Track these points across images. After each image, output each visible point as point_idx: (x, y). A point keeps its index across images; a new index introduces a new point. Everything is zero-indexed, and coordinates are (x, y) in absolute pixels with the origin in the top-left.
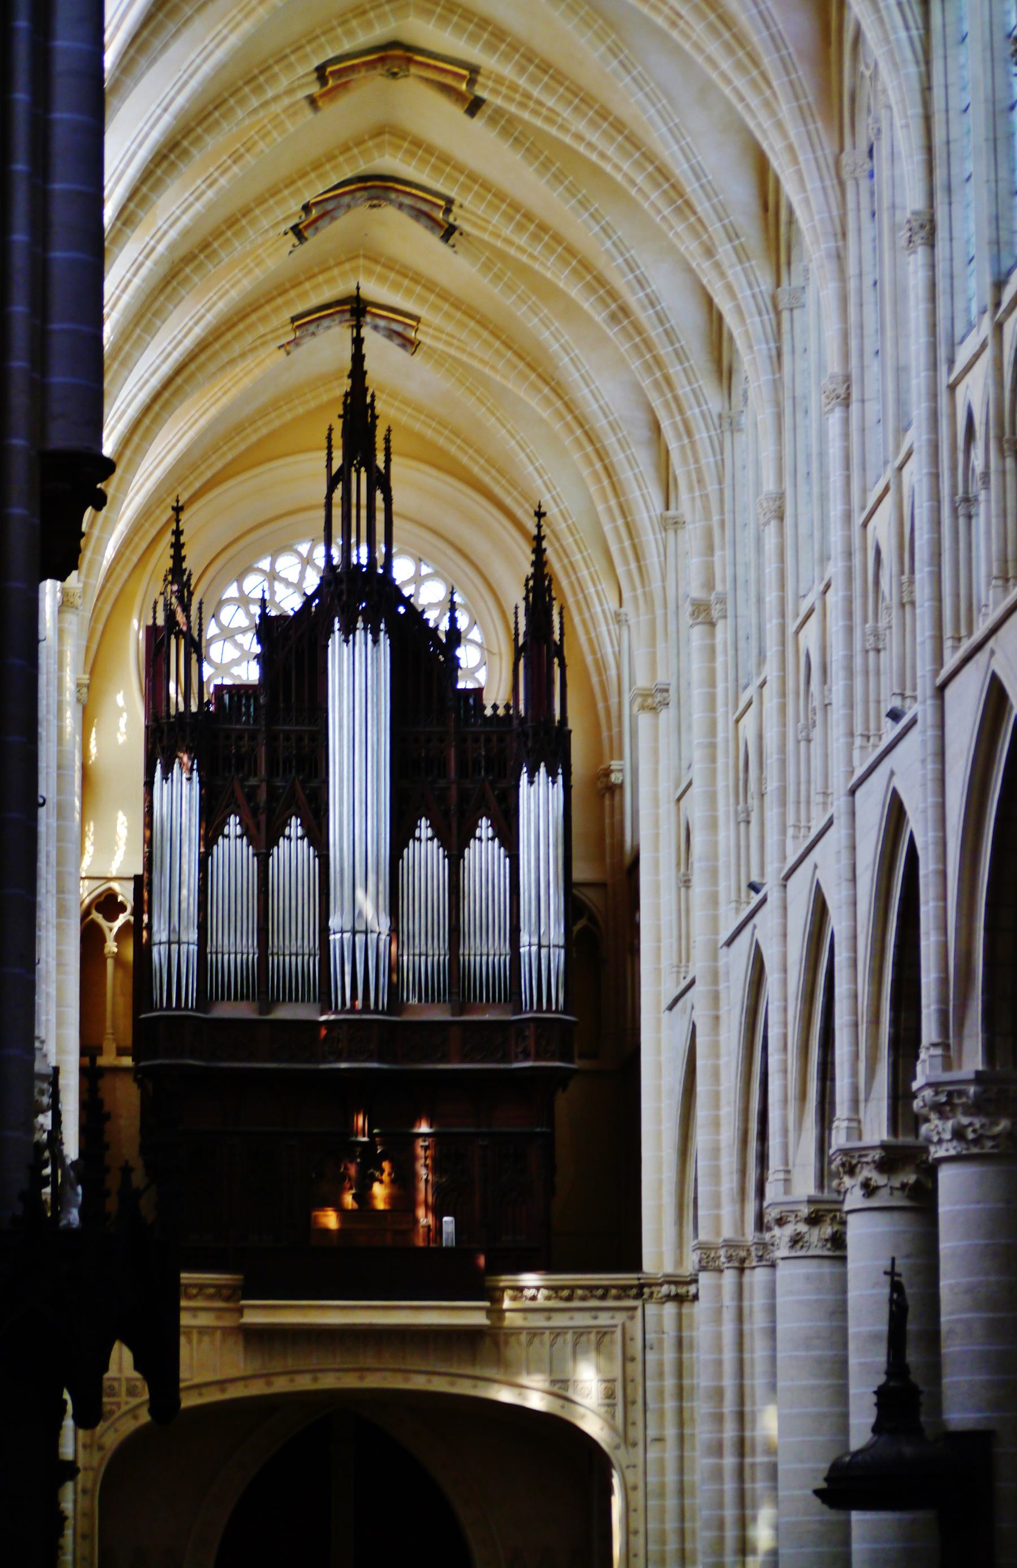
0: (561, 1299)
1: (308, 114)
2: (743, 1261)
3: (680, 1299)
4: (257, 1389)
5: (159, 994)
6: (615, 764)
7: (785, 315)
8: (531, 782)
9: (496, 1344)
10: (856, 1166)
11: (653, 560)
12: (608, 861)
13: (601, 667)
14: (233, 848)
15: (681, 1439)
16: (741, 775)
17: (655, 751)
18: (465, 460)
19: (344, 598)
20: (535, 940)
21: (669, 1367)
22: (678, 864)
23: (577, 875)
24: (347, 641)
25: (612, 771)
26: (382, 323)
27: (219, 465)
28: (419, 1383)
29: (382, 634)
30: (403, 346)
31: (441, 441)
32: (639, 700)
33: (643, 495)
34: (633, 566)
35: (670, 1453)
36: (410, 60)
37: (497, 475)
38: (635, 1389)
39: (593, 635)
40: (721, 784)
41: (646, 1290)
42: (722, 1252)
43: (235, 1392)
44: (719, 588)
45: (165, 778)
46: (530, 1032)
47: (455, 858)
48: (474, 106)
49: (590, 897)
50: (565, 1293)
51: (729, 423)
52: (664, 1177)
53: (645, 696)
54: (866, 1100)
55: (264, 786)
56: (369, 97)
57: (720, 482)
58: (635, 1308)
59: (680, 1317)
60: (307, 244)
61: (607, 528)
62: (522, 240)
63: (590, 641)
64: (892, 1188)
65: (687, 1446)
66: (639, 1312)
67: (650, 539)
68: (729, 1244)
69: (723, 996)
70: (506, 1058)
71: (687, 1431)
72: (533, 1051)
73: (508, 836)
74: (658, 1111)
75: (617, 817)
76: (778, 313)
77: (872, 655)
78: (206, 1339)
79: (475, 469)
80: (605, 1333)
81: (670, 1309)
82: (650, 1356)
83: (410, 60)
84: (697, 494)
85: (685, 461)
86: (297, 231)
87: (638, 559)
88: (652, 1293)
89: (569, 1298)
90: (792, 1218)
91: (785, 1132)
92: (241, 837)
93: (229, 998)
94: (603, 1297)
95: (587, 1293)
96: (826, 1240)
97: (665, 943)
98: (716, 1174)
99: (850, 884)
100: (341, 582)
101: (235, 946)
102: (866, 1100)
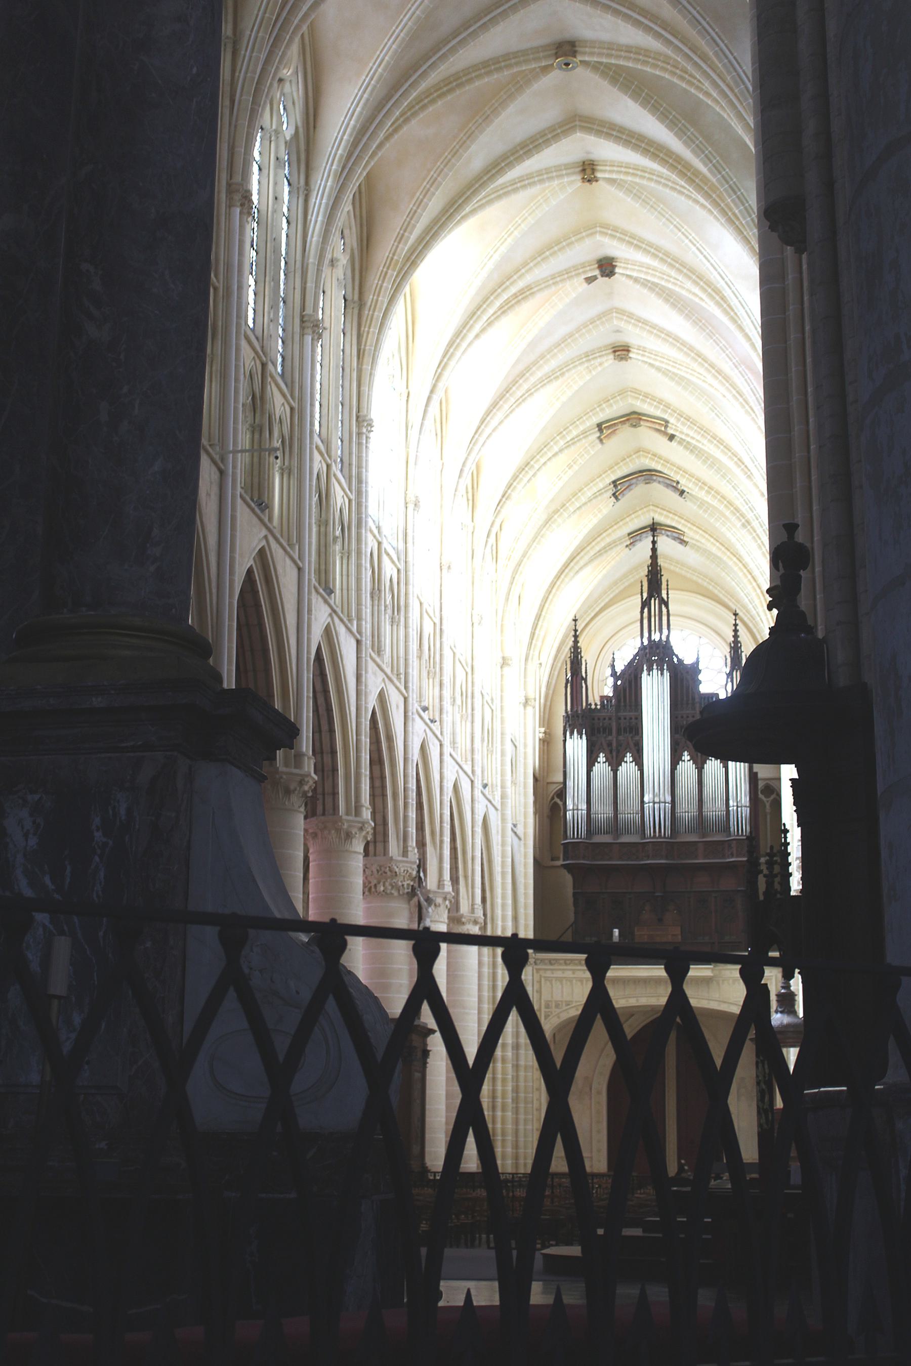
1: (600, 446)
5: (570, 833)
9: (718, 984)
14: (602, 767)
18: (716, 592)
26: (669, 533)
27: (607, 600)
31: (705, 584)
36: (640, 419)
46: (734, 844)
47: (700, 769)
48: (672, 437)
56: (625, 436)
70: (724, 857)
72: (735, 852)
79: (721, 596)
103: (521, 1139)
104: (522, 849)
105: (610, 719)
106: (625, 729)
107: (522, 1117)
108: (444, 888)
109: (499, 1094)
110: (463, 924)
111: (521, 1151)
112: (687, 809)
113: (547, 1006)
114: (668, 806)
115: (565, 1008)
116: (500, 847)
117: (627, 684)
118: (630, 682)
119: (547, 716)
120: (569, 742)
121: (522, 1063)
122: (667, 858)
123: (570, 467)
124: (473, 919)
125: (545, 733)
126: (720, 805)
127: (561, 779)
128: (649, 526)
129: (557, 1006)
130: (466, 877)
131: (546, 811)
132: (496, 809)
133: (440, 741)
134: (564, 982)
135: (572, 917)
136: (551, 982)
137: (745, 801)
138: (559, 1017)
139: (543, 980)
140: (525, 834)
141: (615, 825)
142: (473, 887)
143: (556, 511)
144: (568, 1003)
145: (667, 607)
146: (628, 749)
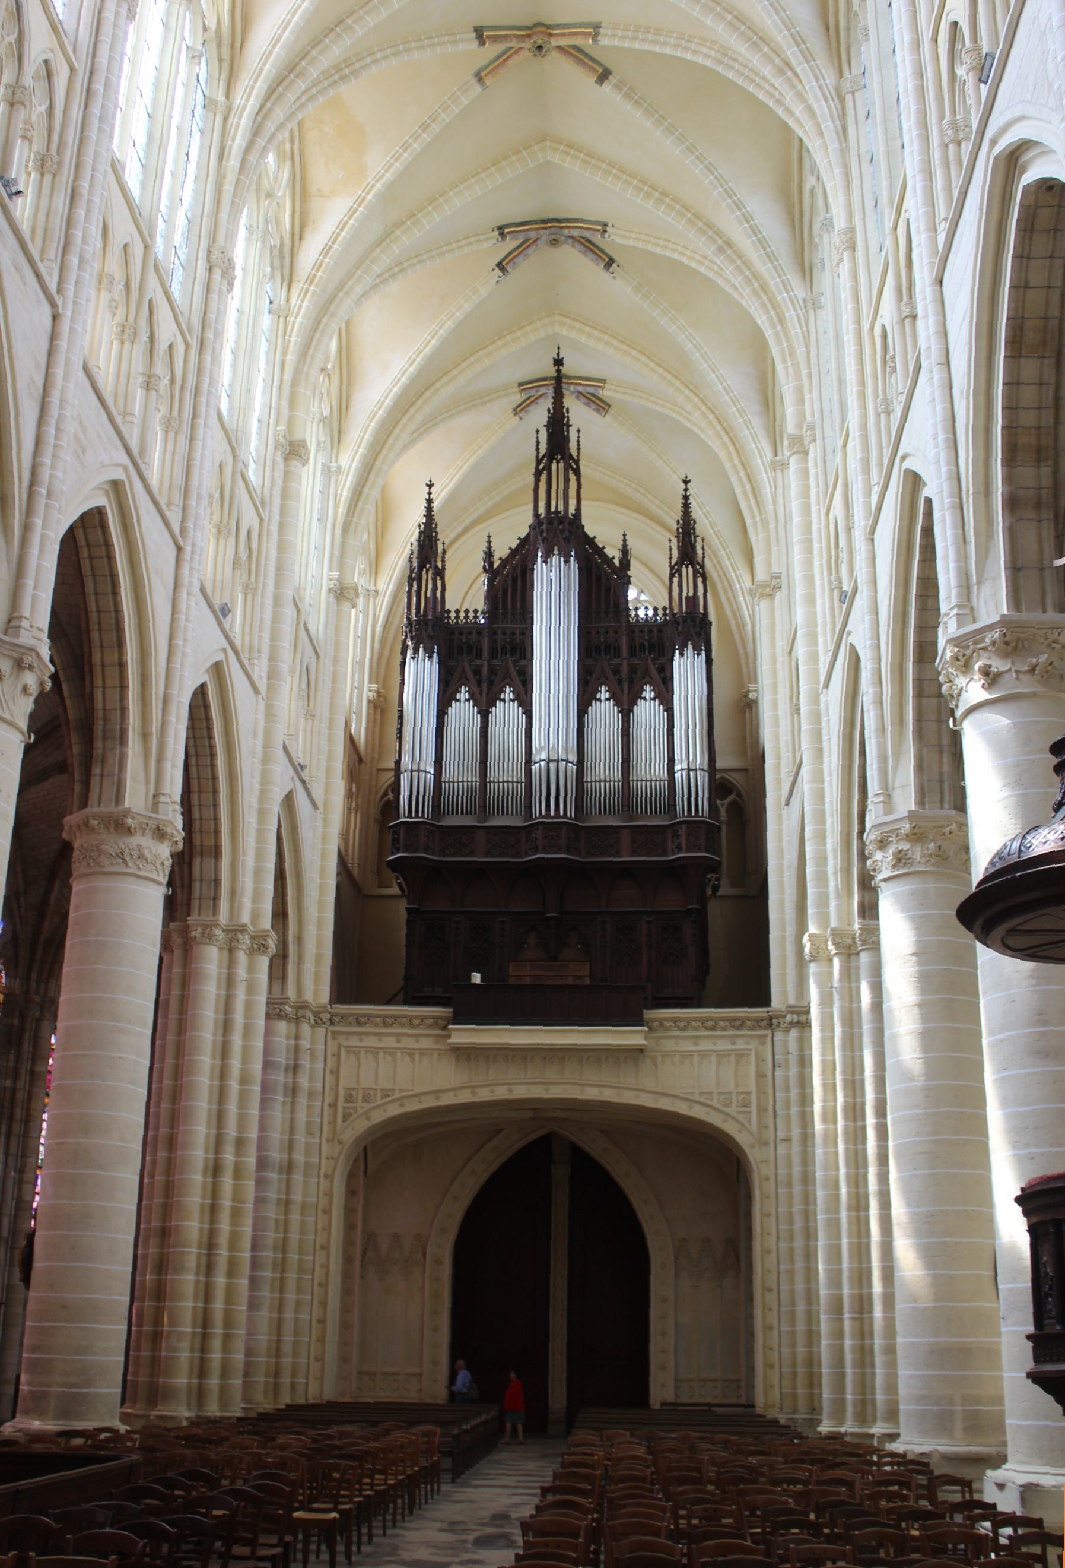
0: (706, 1028)
1: (478, 89)
2: (849, 947)
4: (465, 1097)
6: (752, 687)
7: (849, 98)
8: (682, 655)
10: (971, 656)
11: (767, 492)
12: (749, 753)
13: (741, 625)
14: (463, 712)
17: (773, 625)
20: (685, 766)
21: (793, 1081)
22: (791, 698)
25: (749, 691)
28: (592, 1094)
29: (572, 559)
30: (597, 411)
33: (757, 448)
34: (752, 501)
35: (796, 1148)
36: (550, 35)
39: (735, 607)
40: (816, 563)
41: (774, 1021)
44: (809, 419)
46: (683, 831)
49: (736, 779)
50: (710, 1023)
51: (813, 304)
52: (787, 934)
54: (979, 583)
55: (485, 664)
57: (807, 347)
58: (767, 1036)
60: (509, 277)
62: (650, 204)
63: (733, 611)
64: (1016, 671)
66: (769, 1038)
67: (764, 477)
68: (835, 933)
70: (664, 853)
73: (665, 698)
74: (781, 884)
76: (842, 100)
77: (952, 148)
80: (742, 1055)
81: (794, 1033)
82: (779, 1073)
83: (550, 35)
85: (779, 342)
86: (500, 265)
87: (755, 497)
90: (893, 839)
91: (883, 759)
92: (468, 700)
93: (457, 813)
94: (740, 1027)
95: (727, 1024)
96: (931, 855)
97: (783, 760)
99: (945, 368)
101: (460, 774)
102: (979, 583)
103: (288, 1339)
104: (319, 824)
105: (479, 633)
106: (503, 648)
107: (291, 1296)
108: (17, 636)
109: (223, 1240)
110: (129, 831)
111: (287, 1360)
112: (604, 769)
113: (349, 1099)
114: (572, 768)
115: (379, 1102)
116: (258, 765)
117: (509, 582)
118: (514, 581)
119: (382, 671)
121: (297, 1197)
122: (568, 852)
123: (425, 127)
124: (152, 824)
125: (378, 693)
126: (659, 771)
128: (551, 378)
129: (366, 1098)
130: (145, 736)
131: (374, 811)
132: (256, 691)
133: (53, 305)
134: (381, 1055)
136: (357, 1054)
137: (702, 763)
138: (368, 1119)
139: (343, 1052)
140: (326, 803)
141: (482, 797)
142: (160, 759)
143: (399, 225)
145: (577, 472)
146: (506, 680)
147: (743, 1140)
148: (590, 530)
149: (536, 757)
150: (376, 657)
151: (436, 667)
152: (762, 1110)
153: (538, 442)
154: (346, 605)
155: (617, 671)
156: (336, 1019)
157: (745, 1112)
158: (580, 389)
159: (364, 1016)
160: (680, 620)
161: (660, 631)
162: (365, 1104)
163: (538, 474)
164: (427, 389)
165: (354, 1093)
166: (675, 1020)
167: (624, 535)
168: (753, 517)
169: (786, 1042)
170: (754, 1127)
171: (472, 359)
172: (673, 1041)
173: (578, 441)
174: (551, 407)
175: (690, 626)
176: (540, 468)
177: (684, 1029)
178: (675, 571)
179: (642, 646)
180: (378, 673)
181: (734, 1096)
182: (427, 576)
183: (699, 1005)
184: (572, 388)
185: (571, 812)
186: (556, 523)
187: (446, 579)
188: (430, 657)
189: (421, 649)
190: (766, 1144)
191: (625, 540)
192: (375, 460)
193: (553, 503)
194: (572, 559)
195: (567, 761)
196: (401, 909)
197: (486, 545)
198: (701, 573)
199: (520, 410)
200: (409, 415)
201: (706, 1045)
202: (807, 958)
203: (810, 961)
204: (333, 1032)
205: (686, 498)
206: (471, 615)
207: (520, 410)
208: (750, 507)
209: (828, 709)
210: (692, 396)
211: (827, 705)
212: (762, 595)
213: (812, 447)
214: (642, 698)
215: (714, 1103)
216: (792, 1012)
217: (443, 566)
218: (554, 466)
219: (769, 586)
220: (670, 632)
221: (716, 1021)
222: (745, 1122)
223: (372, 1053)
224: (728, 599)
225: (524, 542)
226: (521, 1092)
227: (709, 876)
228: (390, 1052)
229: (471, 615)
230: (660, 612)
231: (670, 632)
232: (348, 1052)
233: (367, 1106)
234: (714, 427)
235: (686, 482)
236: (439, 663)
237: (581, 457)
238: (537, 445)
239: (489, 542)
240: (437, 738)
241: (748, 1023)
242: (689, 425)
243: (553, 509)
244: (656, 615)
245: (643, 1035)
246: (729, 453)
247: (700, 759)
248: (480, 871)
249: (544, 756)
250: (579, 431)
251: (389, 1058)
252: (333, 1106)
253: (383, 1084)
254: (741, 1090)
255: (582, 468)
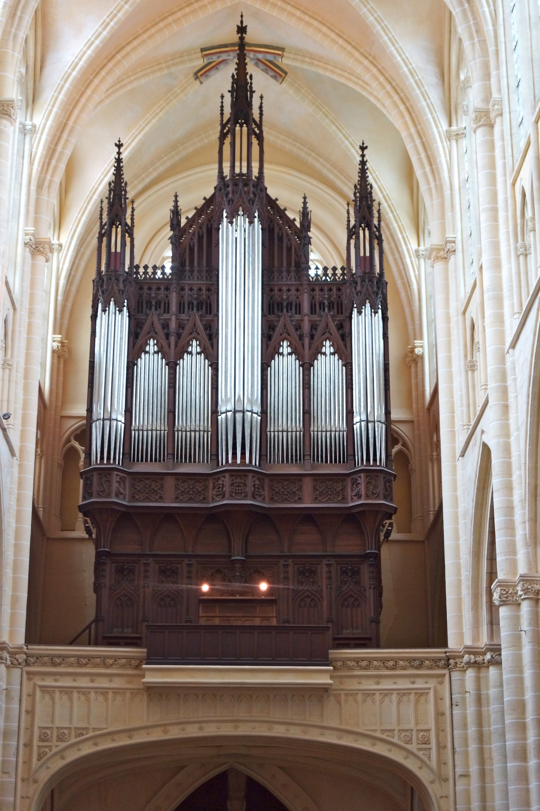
0: (387, 668)
3: (477, 666)
4: (156, 736)
6: (417, 343)
8: (360, 313)
12: (414, 406)
14: (151, 363)
15: (483, 774)
16: (519, 221)
19: (230, 196)
20: (364, 417)
22: (466, 356)
23: (394, 416)
24: (231, 223)
25: (415, 347)
27: (161, 169)
29: (256, 220)
32: (434, 253)
34: (428, 169)
35: (475, 785)
37: (339, 174)
38: (446, 736)
39: (401, 267)
41: (451, 661)
42: (519, 588)
43: (139, 738)
45: (104, 311)
47: (307, 366)
49: (403, 430)
50: (391, 663)
52: (463, 577)
53: (439, 250)
55: (174, 318)
58: (444, 675)
59: (478, 680)
61: (409, 147)
63: (399, 271)
65: (488, 779)
68: (524, 579)
69: (511, 389)
71: (487, 767)
72: (363, 493)
74: (456, 531)
75: (420, 377)
78: (119, 698)
79: (324, 171)
80: (422, 694)
81: (470, 673)
82: (456, 711)
84: (476, 40)
87: (430, 164)
88: (456, 663)
89: (393, 668)
93: (146, 460)
97: (457, 414)
98: (510, 527)
100: (228, 186)
101: (149, 421)
104: (16, 470)
106: (190, 304)
112: (286, 421)
113: (44, 738)
115: (74, 740)
117: (196, 240)
118: (200, 238)
119: (66, 322)
120: (102, 319)
122: (254, 498)
126: (338, 423)
127: (83, 412)
128: (232, 45)
131: (58, 457)
135: (90, 614)
141: (171, 445)
144: (80, 731)
145: (260, 138)
146: (194, 334)
147: (424, 776)
148: (272, 192)
149: (222, 408)
150: (59, 309)
151: (126, 320)
152: (441, 747)
153: (222, 107)
154: (41, 259)
155: (298, 328)
156: (32, 660)
157: (425, 749)
158: (260, 56)
159: (59, 656)
160: (359, 280)
161: (339, 290)
162: (59, 743)
163: (222, 137)
164: (118, 52)
165: (48, 732)
166: (357, 660)
167: (305, 198)
168: (428, 183)
169: (463, 681)
170: (434, 763)
171: (161, 25)
172: (356, 680)
173: (261, 108)
174: (235, 73)
175: (368, 284)
176: (225, 131)
177: (366, 668)
178: (352, 233)
179: (322, 304)
180: (61, 324)
181: (414, 733)
182: (117, 233)
183: (378, 646)
184: (251, 55)
185: (256, 460)
186: (241, 185)
187: (135, 236)
188: (121, 311)
189: (112, 303)
190: (446, 780)
191: (305, 203)
192: (68, 119)
193: (237, 164)
194: (256, 220)
195: (252, 412)
196: (88, 553)
197: (173, 204)
198: (377, 237)
199: (200, 74)
200: (100, 77)
201: (386, 685)
202: (497, 603)
203: (500, 606)
204: (28, 673)
205: (363, 163)
206: (150, 270)
207: (200, 74)
208: (425, 174)
209: (514, 368)
210: (371, 67)
211: (513, 363)
212: (437, 258)
213: (498, 120)
214: (322, 353)
215: (395, 740)
216: (469, 653)
217: (132, 222)
218: (238, 128)
219: (444, 250)
220: (348, 290)
221: (396, 660)
222: (425, 759)
223: (66, 693)
224: (395, 260)
225: (209, 202)
226: (211, 730)
227: (386, 521)
228: (84, 691)
229: (150, 270)
230: (330, 272)
231: (348, 290)
232: (43, 691)
233: (63, 745)
234: (390, 97)
235: (363, 148)
236: (129, 316)
237: (264, 123)
238: (222, 110)
239: (176, 201)
240: (126, 386)
241: (427, 662)
242: (365, 94)
243: (237, 171)
244: (325, 274)
245: (328, 675)
246: (405, 122)
247: (379, 413)
248: (169, 516)
249: (230, 407)
250: (262, 97)
251: (83, 698)
252: (28, 745)
253: (77, 723)
254: (420, 727)
255: (265, 134)
